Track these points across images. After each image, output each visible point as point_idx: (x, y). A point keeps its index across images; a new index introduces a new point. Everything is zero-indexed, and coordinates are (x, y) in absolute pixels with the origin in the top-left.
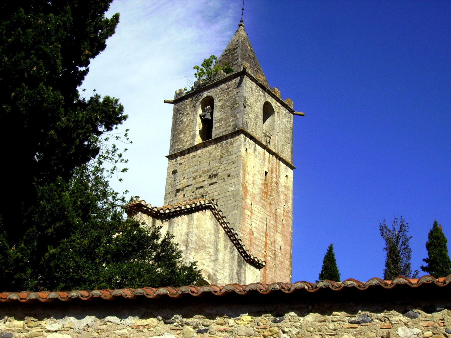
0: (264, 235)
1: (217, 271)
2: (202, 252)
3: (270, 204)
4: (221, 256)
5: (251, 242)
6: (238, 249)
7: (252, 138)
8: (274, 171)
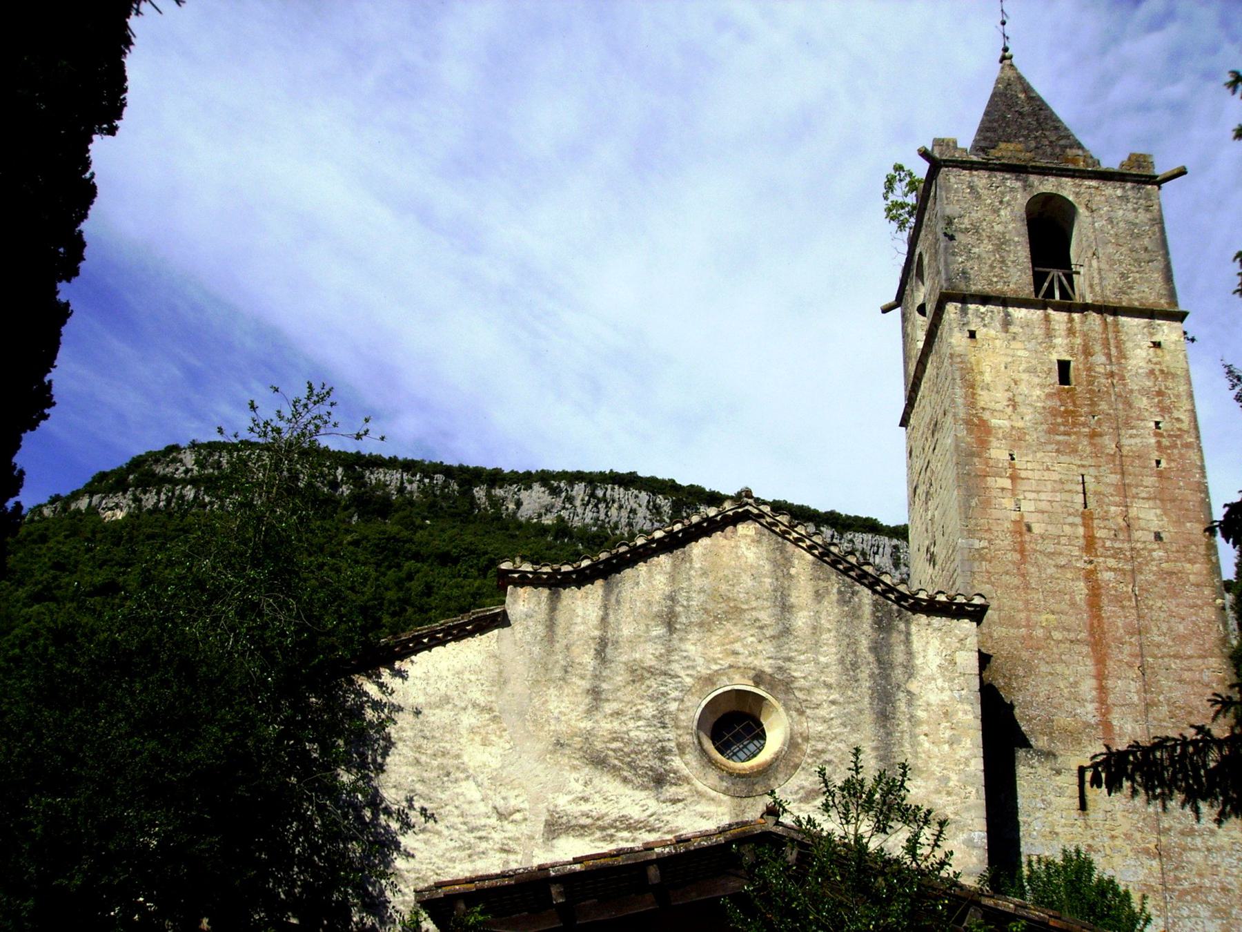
0: (1078, 520)
1: (789, 659)
2: (729, 625)
3: (1093, 435)
4: (801, 620)
5: (1022, 552)
6: (871, 586)
7: (985, 299)
8: (1098, 348)
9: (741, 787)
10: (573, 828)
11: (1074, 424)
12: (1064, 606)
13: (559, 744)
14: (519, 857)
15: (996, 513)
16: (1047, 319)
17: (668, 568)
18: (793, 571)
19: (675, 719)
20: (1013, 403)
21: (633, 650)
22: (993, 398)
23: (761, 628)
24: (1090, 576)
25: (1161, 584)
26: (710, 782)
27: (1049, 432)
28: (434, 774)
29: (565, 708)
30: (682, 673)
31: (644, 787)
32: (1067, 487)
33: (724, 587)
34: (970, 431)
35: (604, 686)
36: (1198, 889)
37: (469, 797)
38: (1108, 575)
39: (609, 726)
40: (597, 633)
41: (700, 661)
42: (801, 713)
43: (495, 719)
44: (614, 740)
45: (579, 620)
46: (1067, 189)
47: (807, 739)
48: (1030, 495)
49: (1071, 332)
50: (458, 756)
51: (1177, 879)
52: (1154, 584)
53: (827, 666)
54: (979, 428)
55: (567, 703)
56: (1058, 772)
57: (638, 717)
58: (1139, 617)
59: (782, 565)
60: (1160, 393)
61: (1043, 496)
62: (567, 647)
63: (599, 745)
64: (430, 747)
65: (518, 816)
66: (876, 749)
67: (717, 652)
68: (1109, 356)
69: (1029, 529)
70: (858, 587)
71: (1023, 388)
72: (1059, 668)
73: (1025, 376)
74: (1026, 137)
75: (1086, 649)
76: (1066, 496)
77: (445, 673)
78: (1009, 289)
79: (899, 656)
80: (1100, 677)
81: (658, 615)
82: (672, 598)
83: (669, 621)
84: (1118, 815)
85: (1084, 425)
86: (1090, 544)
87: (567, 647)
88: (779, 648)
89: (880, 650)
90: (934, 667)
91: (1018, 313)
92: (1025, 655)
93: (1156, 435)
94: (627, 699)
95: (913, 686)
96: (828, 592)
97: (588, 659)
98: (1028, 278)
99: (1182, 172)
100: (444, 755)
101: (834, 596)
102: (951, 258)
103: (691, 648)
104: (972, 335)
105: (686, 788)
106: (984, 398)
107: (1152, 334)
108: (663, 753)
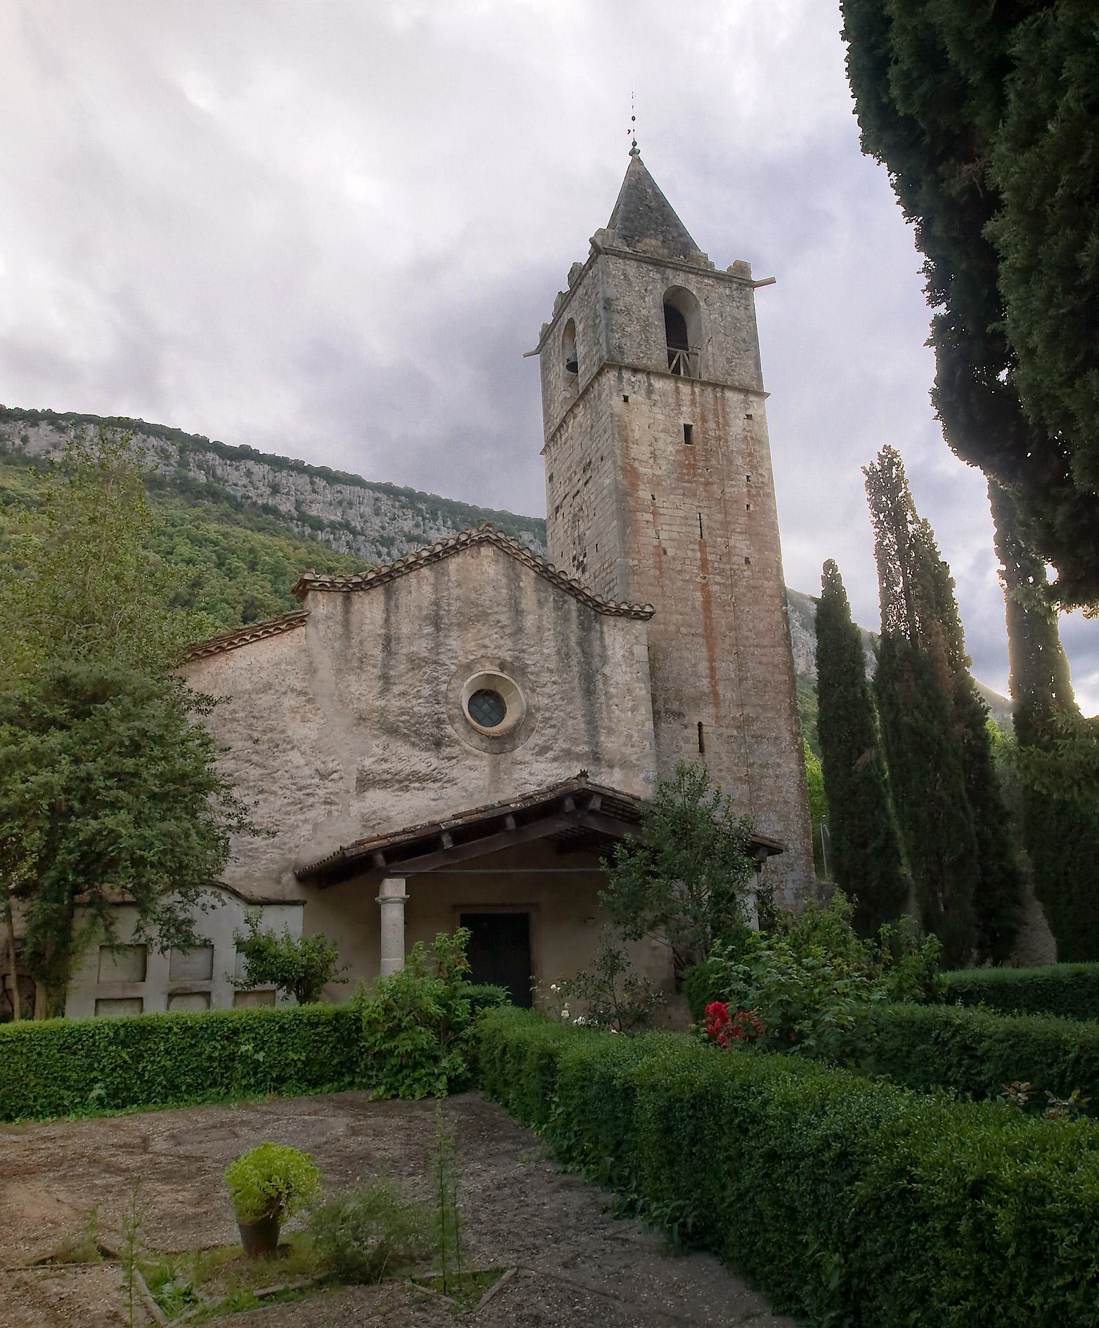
0: (697, 547)
1: (523, 651)
2: (479, 626)
3: (707, 484)
4: (529, 622)
5: (660, 569)
6: (575, 596)
7: (635, 370)
8: (710, 416)
9: (496, 747)
10: (378, 782)
11: (695, 475)
12: (688, 610)
13: (362, 719)
14: (340, 807)
15: (643, 540)
16: (677, 390)
17: (432, 580)
18: (522, 584)
19: (446, 697)
20: (654, 456)
21: (411, 644)
22: (640, 451)
23: (502, 627)
24: (704, 588)
25: (749, 595)
26: (474, 743)
27: (678, 479)
28: (265, 747)
29: (363, 689)
30: (448, 662)
31: (427, 749)
32: (690, 522)
33: (474, 596)
34: (625, 477)
35: (392, 673)
36: (770, 802)
37: (296, 763)
38: (716, 588)
39: (398, 704)
40: (383, 631)
41: (461, 653)
42: (533, 691)
43: (309, 701)
44: (402, 714)
45: (368, 621)
46: (692, 284)
47: (538, 710)
48: (665, 527)
49: (693, 403)
50: (283, 732)
51: (758, 796)
52: (744, 595)
53: (549, 656)
54: (630, 472)
55: (364, 687)
56: (686, 727)
57: (418, 696)
58: (736, 618)
59: (513, 580)
60: (750, 454)
61: (674, 528)
62: (361, 643)
63: (392, 719)
64: (260, 725)
65: (335, 776)
66: (583, 716)
67: (471, 646)
68: (718, 423)
69: (665, 553)
70: (567, 597)
71: (661, 445)
72: (685, 654)
73: (662, 435)
74: (656, 230)
75: (702, 640)
76: (689, 529)
77: (265, 665)
78: (651, 364)
79: (597, 649)
80: (711, 660)
81: (426, 617)
82: (436, 604)
83: (436, 622)
84: (723, 755)
85: (701, 475)
86: (704, 564)
87: (361, 643)
88: (515, 643)
89: (584, 643)
90: (619, 656)
91: (658, 384)
92: (663, 644)
93: (747, 486)
94: (410, 682)
95: (607, 670)
96: (546, 600)
97: (377, 652)
98: (664, 355)
99: (772, 281)
100: (271, 730)
101: (551, 604)
102: (610, 334)
103: (453, 643)
104: (626, 399)
105: (458, 748)
106: (635, 451)
107: (747, 409)
108: (439, 723)
